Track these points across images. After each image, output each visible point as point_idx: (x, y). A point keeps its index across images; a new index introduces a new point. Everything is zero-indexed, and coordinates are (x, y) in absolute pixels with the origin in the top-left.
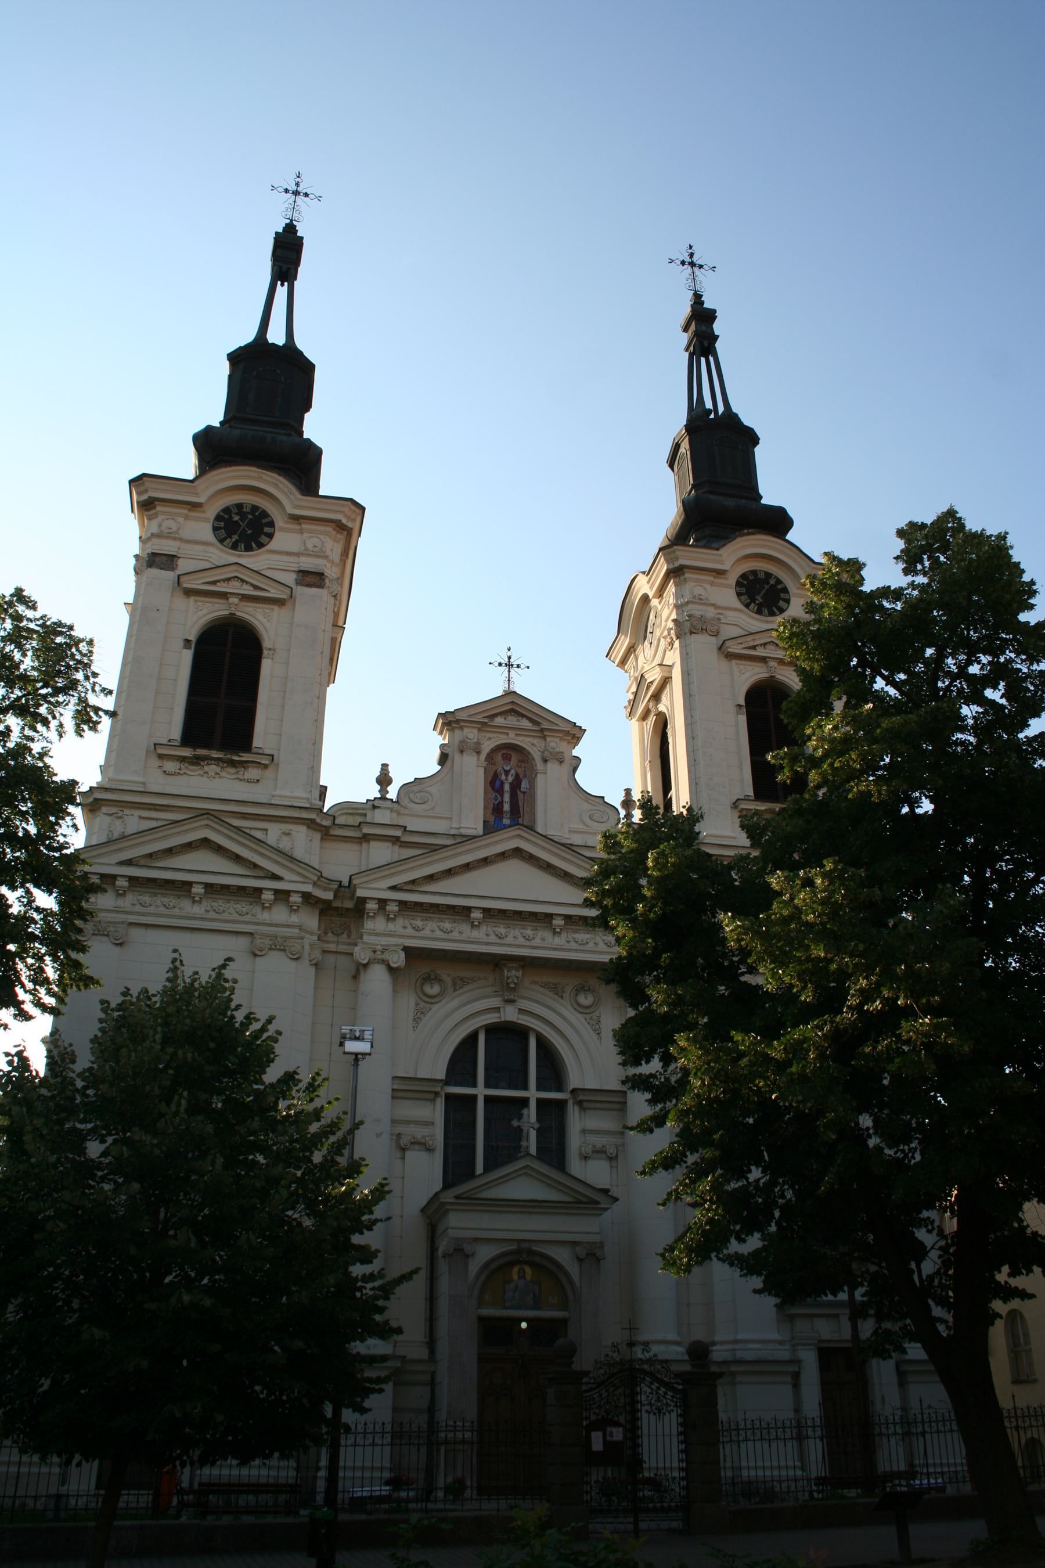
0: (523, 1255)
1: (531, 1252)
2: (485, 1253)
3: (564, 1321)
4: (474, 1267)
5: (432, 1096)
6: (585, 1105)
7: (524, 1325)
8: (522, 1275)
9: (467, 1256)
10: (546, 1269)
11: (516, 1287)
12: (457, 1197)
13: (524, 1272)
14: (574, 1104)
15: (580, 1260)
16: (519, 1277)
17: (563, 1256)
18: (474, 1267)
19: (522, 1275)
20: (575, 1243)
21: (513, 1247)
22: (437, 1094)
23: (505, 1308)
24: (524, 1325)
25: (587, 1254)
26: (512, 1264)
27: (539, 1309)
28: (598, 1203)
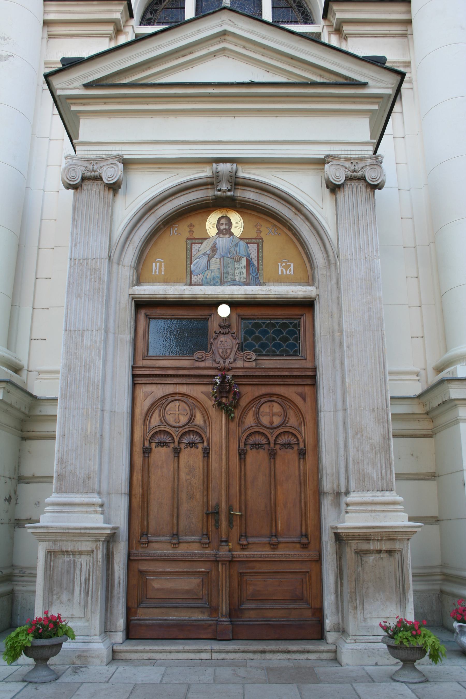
0: (225, 192)
1: (236, 183)
2: (146, 187)
3: (308, 305)
4: (126, 208)
5: (110, 29)
6: (347, 29)
7: (224, 311)
8: (225, 229)
9: (114, 187)
10: (272, 215)
11: (214, 249)
12: (87, 86)
13: (230, 223)
14: (329, 34)
15: (334, 188)
16: (220, 232)
17: (303, 187)
18: (126, 208)
19: (225, 229)
20: (322, 162)
21: (204, 173)
22: (118, 31)
23: (191, 284)
24: (224, 311)
25: (349, 179)
26: (203, 208)
27: (259, 284)
28: (364, 85)
